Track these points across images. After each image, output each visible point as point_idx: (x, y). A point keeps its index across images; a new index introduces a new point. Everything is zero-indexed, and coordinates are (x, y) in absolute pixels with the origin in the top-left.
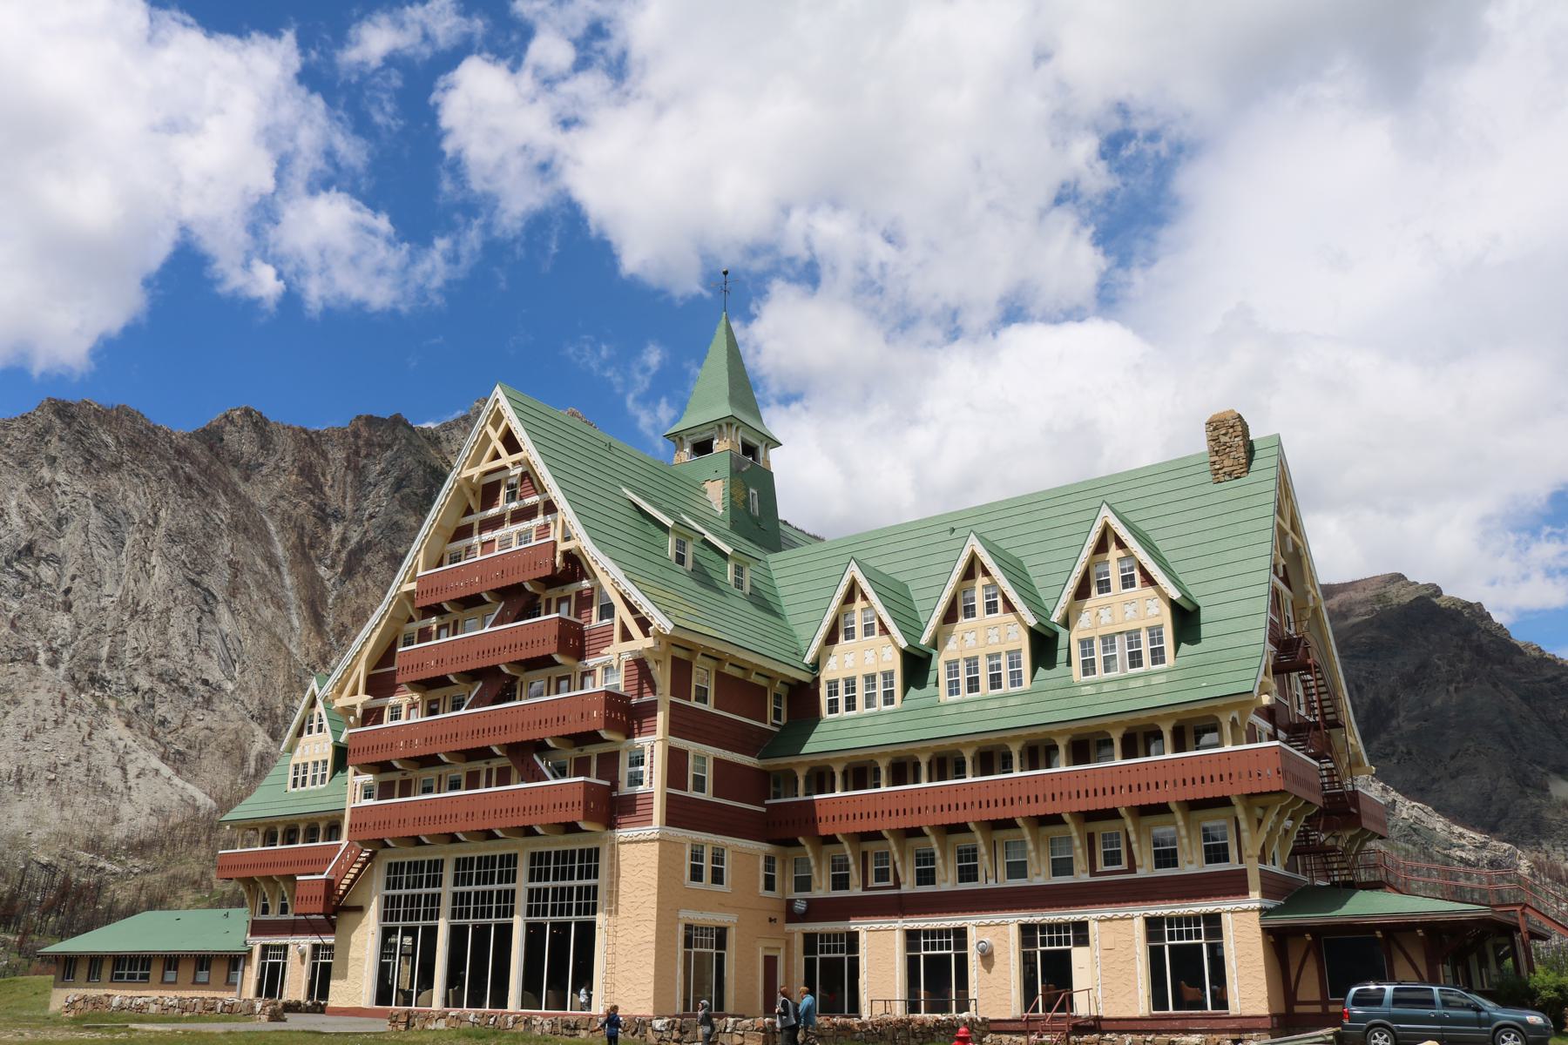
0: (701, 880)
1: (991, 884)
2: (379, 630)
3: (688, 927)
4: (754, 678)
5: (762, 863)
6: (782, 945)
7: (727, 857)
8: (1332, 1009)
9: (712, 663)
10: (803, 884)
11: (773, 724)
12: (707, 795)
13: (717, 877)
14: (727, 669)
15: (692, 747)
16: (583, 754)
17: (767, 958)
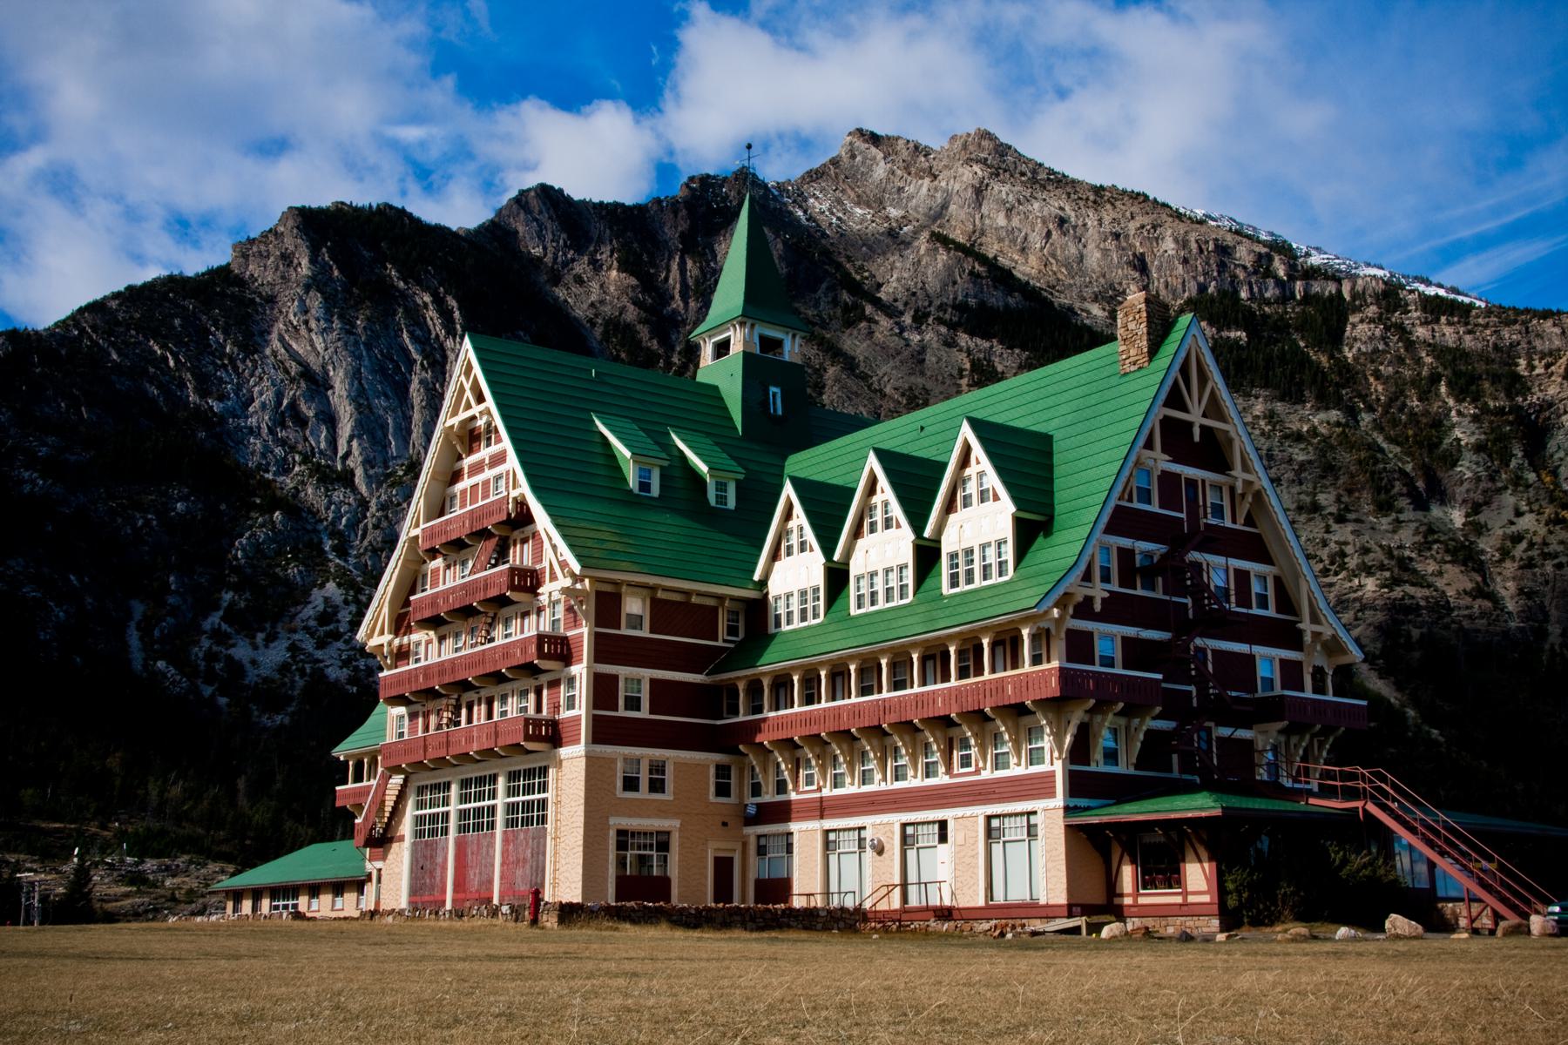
0: (636, 789)
1: (883, 787)
2: (397, 571)
3: (621, 833)
4: (694, 599)
5: (712, 771)
6: (739, 847)
7: (669, 769)
8: (1142, 900)
9: (645, 592)
10: (756, 790)
11: (725, 641)
12: (644, 713)
13: (657, 786)
14: (660, 595)
15: (623, 671)
16: (537, 683)
17: (717, 860)
